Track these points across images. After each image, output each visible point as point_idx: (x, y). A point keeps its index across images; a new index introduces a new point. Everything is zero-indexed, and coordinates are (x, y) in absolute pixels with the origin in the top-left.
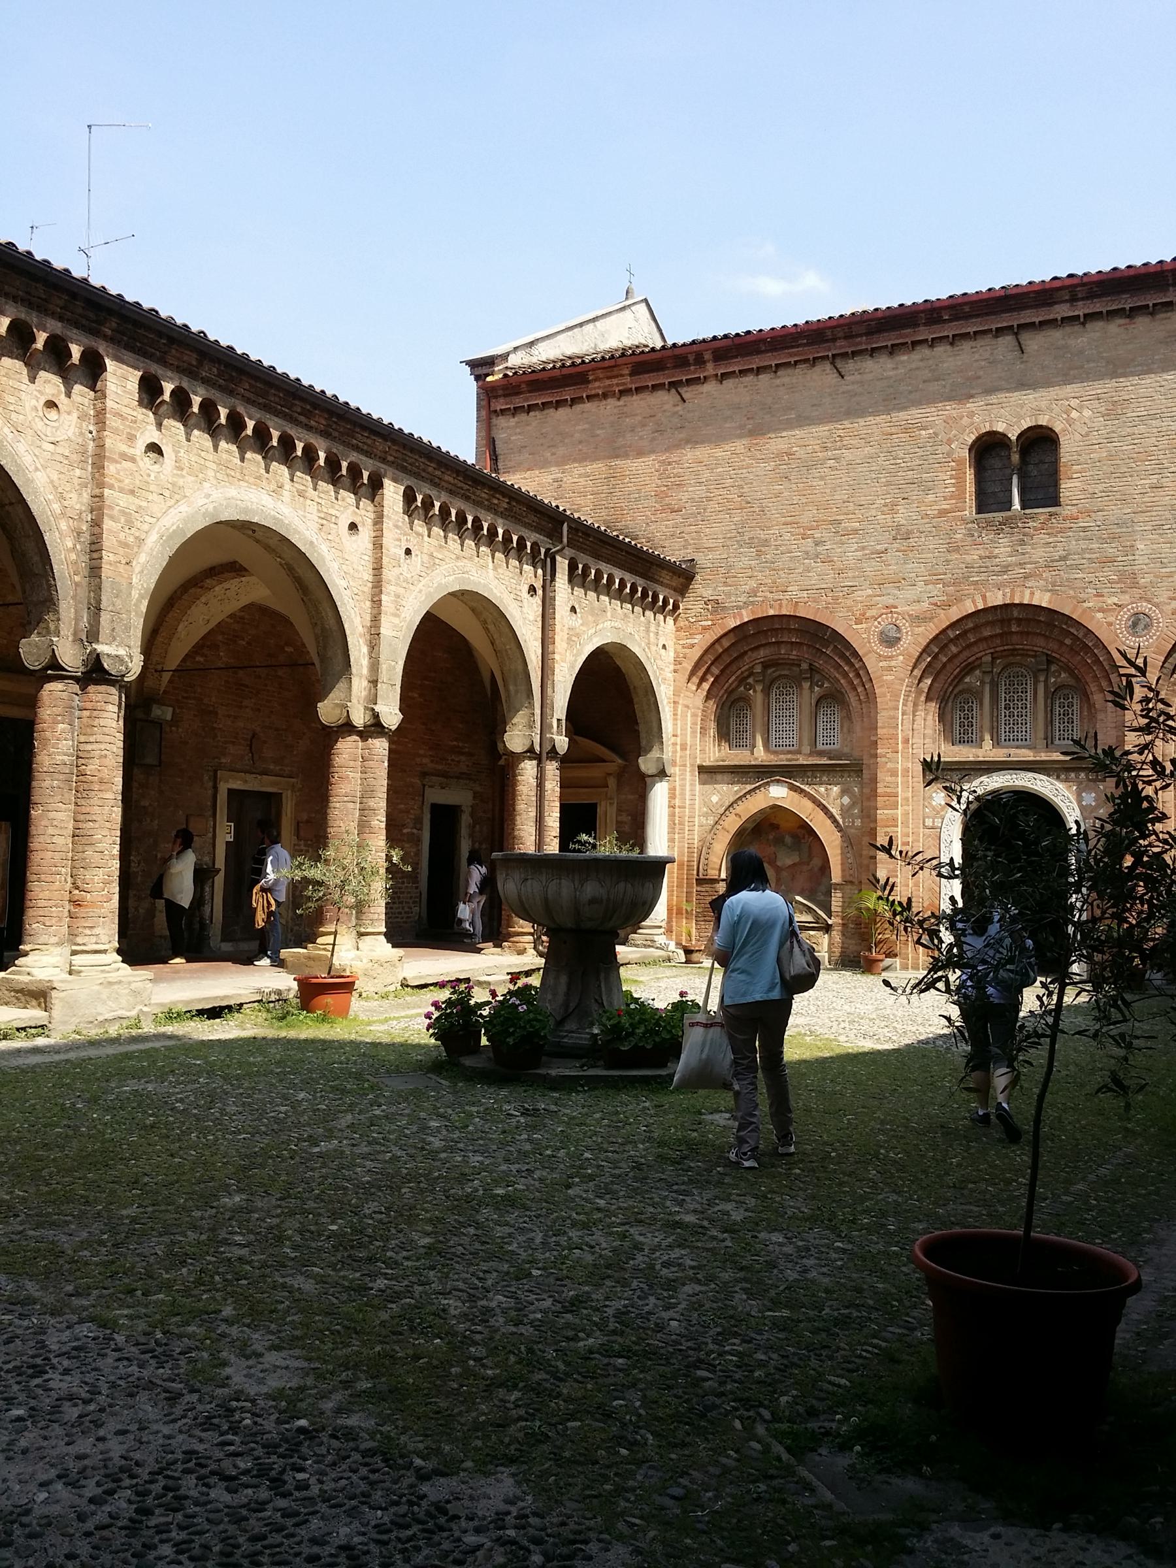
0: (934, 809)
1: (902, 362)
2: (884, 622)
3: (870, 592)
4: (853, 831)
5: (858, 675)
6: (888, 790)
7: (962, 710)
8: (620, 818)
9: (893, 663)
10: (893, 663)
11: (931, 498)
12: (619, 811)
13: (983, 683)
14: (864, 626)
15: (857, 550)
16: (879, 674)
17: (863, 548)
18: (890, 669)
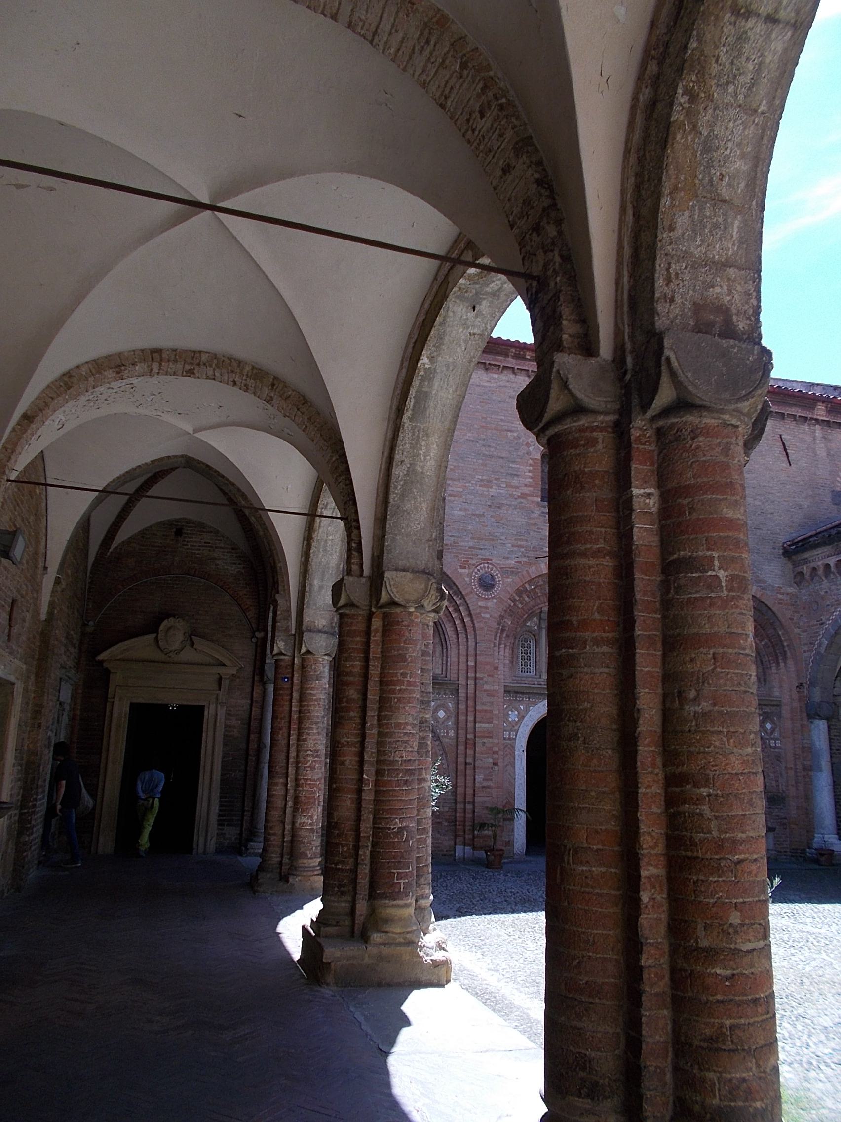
0: (510, 723)
1: (494, 379)
2: (483, 569)
3: (471, 544)
4: (447, 740)
5: (457, 610)
6: (485, 708)
7: (523, 646)
8: (228, 722)
9: (489, 604)
10: (489, 604)
11: (515, 482)
12: (229, 714)
13: (540, 628)
14: (467, 571)
15: (460, 510)
16: (478, 611)
17: (466, 510)
18: (487, 608)
